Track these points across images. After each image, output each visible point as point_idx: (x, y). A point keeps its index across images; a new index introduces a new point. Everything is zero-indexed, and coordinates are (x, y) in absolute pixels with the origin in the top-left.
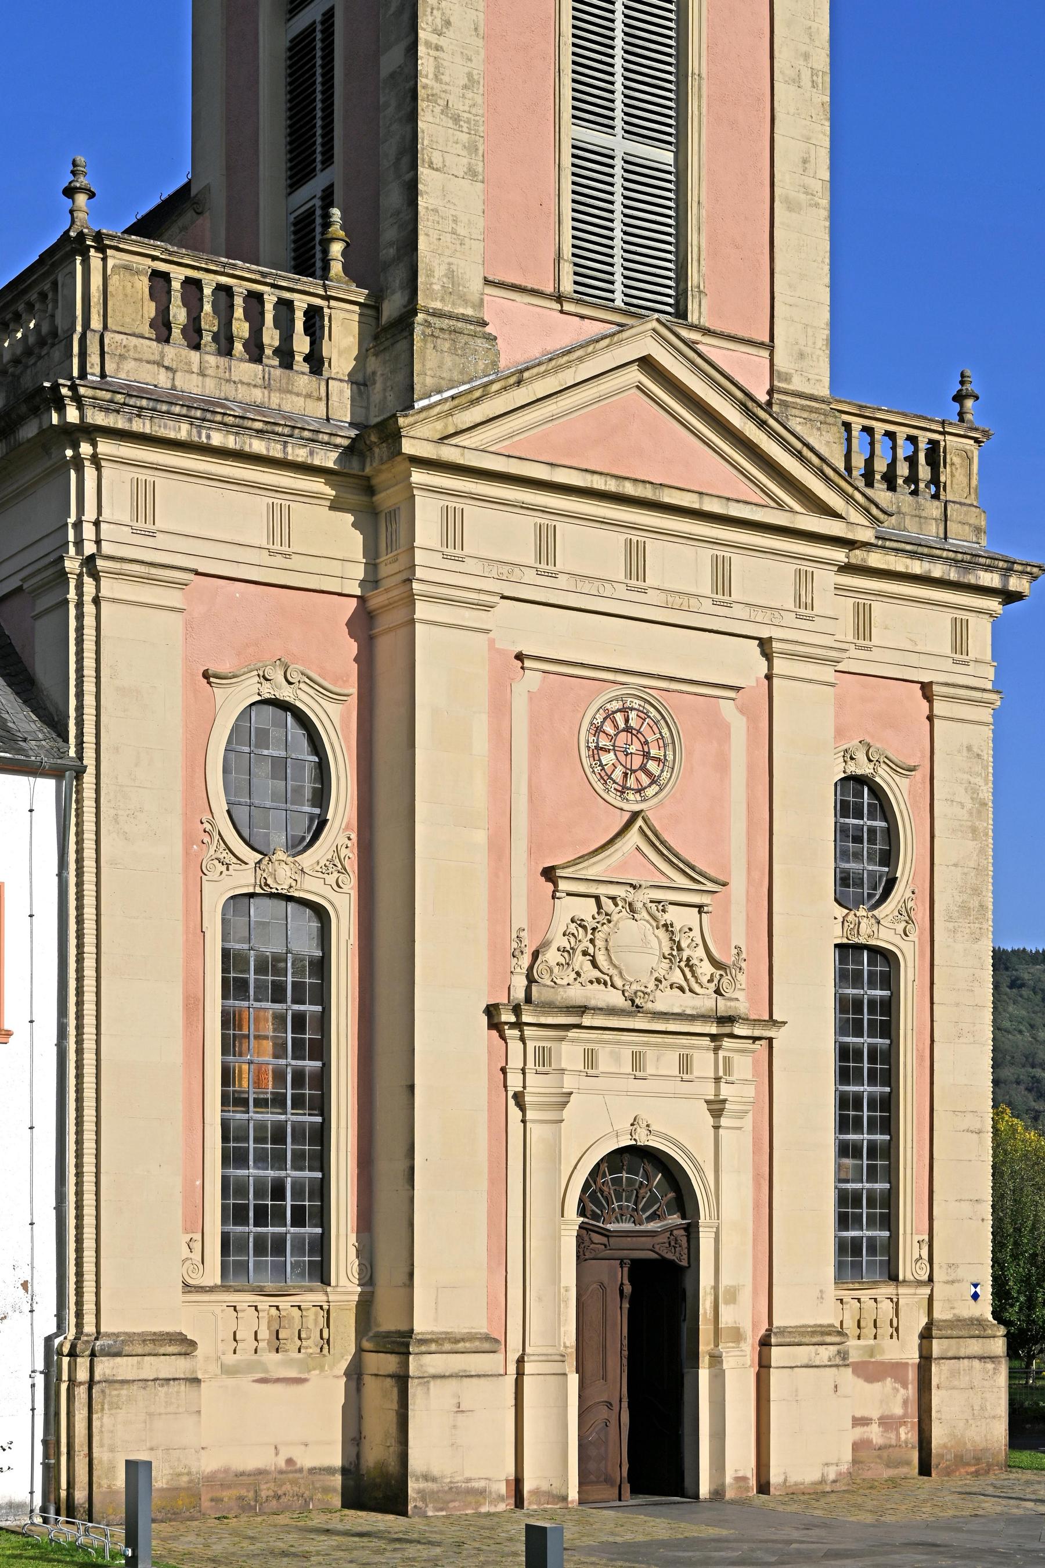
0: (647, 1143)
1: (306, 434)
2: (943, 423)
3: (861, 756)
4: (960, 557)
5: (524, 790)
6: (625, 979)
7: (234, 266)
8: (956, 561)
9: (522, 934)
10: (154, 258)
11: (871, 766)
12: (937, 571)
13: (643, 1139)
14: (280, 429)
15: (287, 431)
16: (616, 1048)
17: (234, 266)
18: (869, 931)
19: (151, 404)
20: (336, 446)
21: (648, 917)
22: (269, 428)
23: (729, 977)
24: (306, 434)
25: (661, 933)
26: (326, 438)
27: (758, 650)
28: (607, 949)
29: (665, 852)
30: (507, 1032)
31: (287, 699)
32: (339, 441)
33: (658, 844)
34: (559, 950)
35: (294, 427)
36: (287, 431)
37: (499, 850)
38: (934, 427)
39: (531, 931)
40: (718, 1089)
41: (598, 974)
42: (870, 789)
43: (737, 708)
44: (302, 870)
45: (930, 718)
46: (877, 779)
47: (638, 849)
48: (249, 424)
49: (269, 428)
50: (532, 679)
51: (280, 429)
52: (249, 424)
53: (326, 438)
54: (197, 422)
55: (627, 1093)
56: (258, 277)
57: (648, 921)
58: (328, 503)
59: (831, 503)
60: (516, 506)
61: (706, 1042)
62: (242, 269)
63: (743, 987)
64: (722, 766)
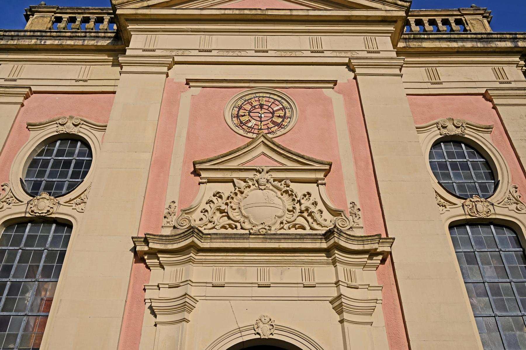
0: (271, 337)
1: (93, 34)
2: (459, 10)
3: (450, 126)
4: (479, 36)
5: (184, 134)
6: (253, 224)
7: (88, 9)
8: (479, 39)
9: (173, 205)
10: (55, 13)
11: (459, 130)
12: (469, 45)
13: (266, 333)
14: (79, 34)
15: (83, 34)
16: (242, 267)
17: (88, 9)
18: (485, 209)
19: (16, 33)
20: (109, 37)
21: (271, 187)
22: (74, 34)
23: (344, 217)
24: (93, 34)
25: (285, 197)
26: (103, 34)
27: (347, 69)
28: (239, 208)
29: (282, 151)
30: (147, 261)
31: (74, 132)
32: (109, 35)
33: (276, 148)
34: (202, 212)
35: (86, 32)
36: (83, 34)
37: (160, 164)
38: (455, 13)
39: (180, 202)
40: (339, 290)
41: (231, 222)
42: (465, 145)
43: (336, 92)
44: (58, 203)
45: (494, 108)
46: (466, 136)
47: (264, 154)
48: (64, 34)
49: (74, 34)
50: (196, 91)
51: (79, 34)
52: (64, 34)
53: (103, 34)
54: (40, 38)
55: (253, 298)
56: (100, 11)
57: (272, 190)
58: (111, 63)
59: (374, 6)
60: (188, 31)
61: (322, 257)
62: (92, 9)
63: (361, 226)
64: (329, 115)
